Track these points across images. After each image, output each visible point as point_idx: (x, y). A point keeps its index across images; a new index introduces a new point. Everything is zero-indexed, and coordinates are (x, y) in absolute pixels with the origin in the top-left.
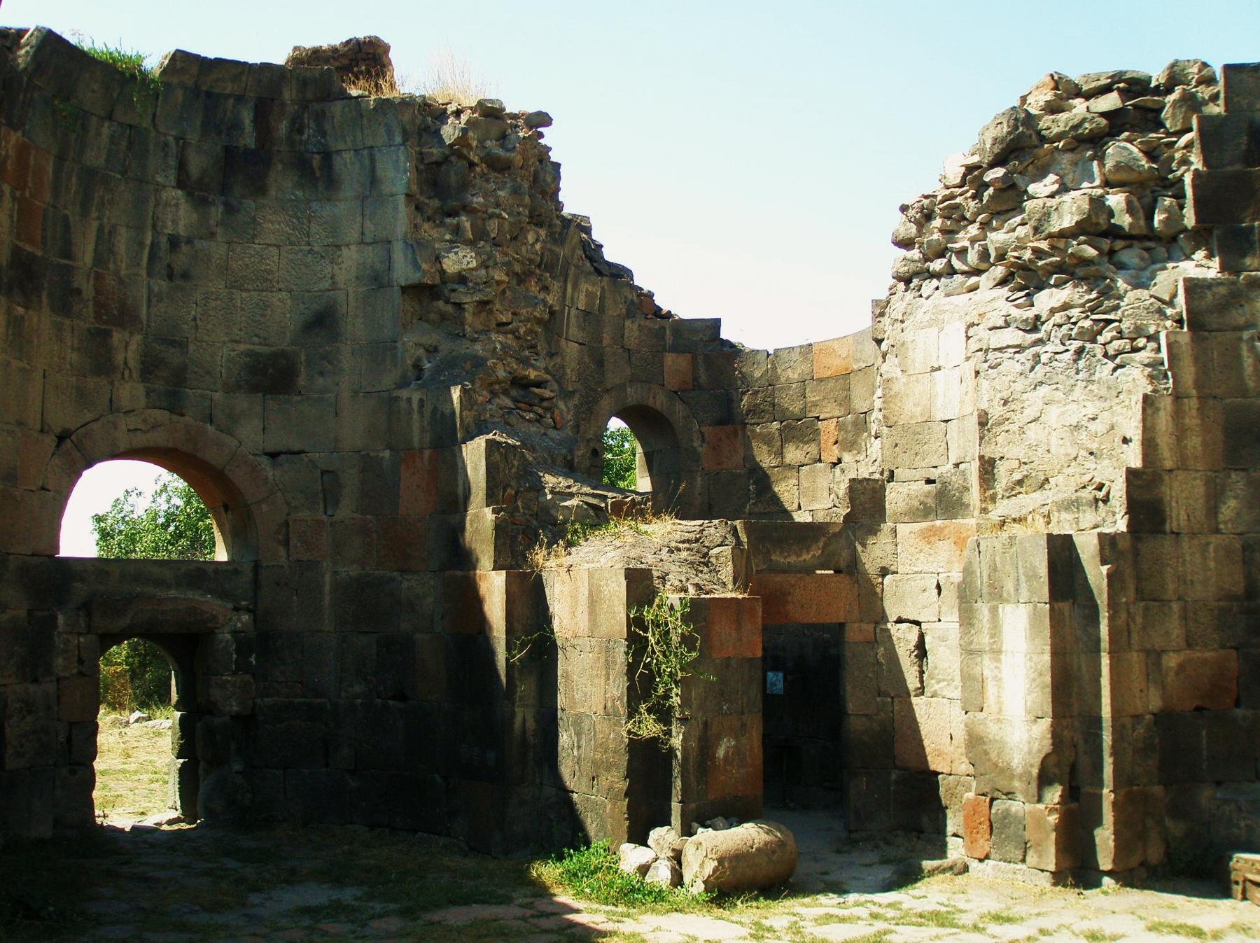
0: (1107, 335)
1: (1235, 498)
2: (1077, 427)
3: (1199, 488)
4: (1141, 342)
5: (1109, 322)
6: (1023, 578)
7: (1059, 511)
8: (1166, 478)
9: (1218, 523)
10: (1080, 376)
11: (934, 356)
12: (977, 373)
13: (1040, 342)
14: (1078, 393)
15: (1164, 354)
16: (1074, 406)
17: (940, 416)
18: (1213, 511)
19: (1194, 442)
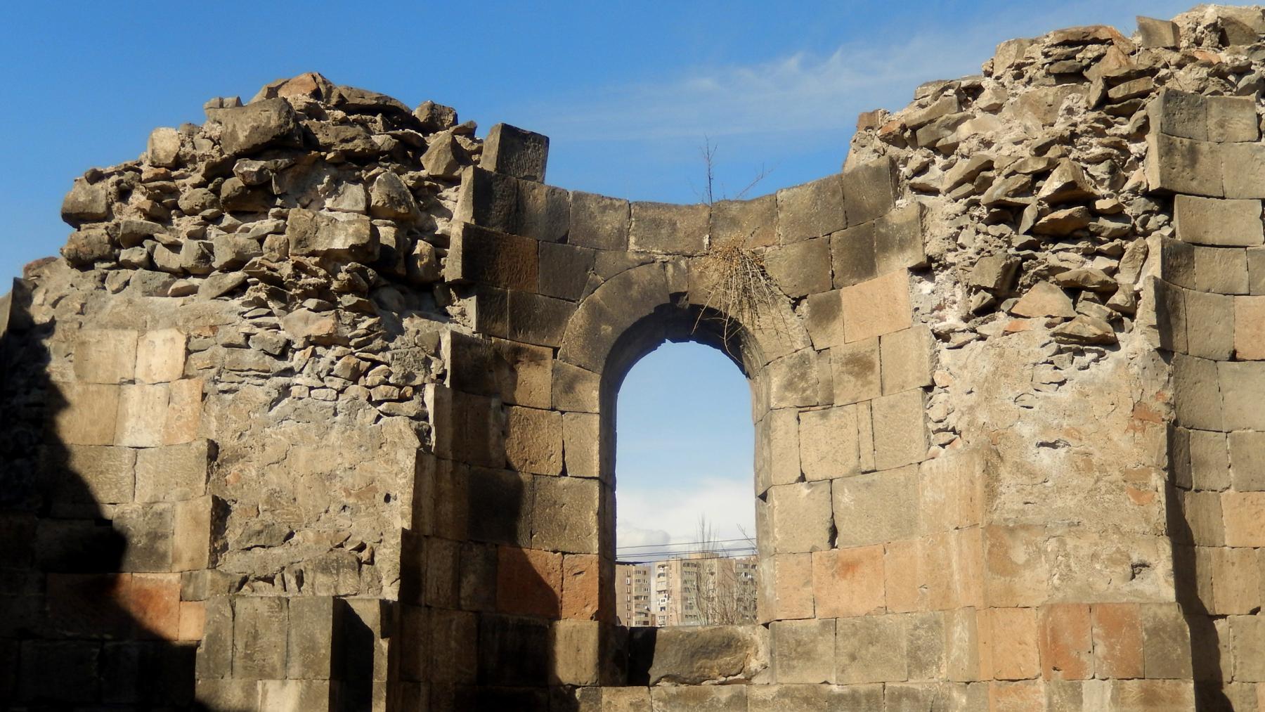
0: (374, 376)
1: (474, 572)
2: (331, 476)
3: (449, 562)
4: (408, 391)
5: (375, 363)
6: (295, 650)
7: (314, 571)
8: (425, 545)
9: (459, 598)
10: (338, 418)
11: (130, 366)
12: (204, 395)
13: (289, 372)
14: (334, 436)
15: (430, 408)
16: (328, 452)
17: (128, 440)
18: (457, 585)
19: (447, 508)
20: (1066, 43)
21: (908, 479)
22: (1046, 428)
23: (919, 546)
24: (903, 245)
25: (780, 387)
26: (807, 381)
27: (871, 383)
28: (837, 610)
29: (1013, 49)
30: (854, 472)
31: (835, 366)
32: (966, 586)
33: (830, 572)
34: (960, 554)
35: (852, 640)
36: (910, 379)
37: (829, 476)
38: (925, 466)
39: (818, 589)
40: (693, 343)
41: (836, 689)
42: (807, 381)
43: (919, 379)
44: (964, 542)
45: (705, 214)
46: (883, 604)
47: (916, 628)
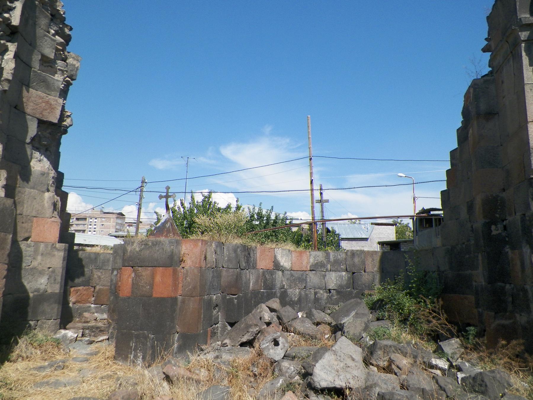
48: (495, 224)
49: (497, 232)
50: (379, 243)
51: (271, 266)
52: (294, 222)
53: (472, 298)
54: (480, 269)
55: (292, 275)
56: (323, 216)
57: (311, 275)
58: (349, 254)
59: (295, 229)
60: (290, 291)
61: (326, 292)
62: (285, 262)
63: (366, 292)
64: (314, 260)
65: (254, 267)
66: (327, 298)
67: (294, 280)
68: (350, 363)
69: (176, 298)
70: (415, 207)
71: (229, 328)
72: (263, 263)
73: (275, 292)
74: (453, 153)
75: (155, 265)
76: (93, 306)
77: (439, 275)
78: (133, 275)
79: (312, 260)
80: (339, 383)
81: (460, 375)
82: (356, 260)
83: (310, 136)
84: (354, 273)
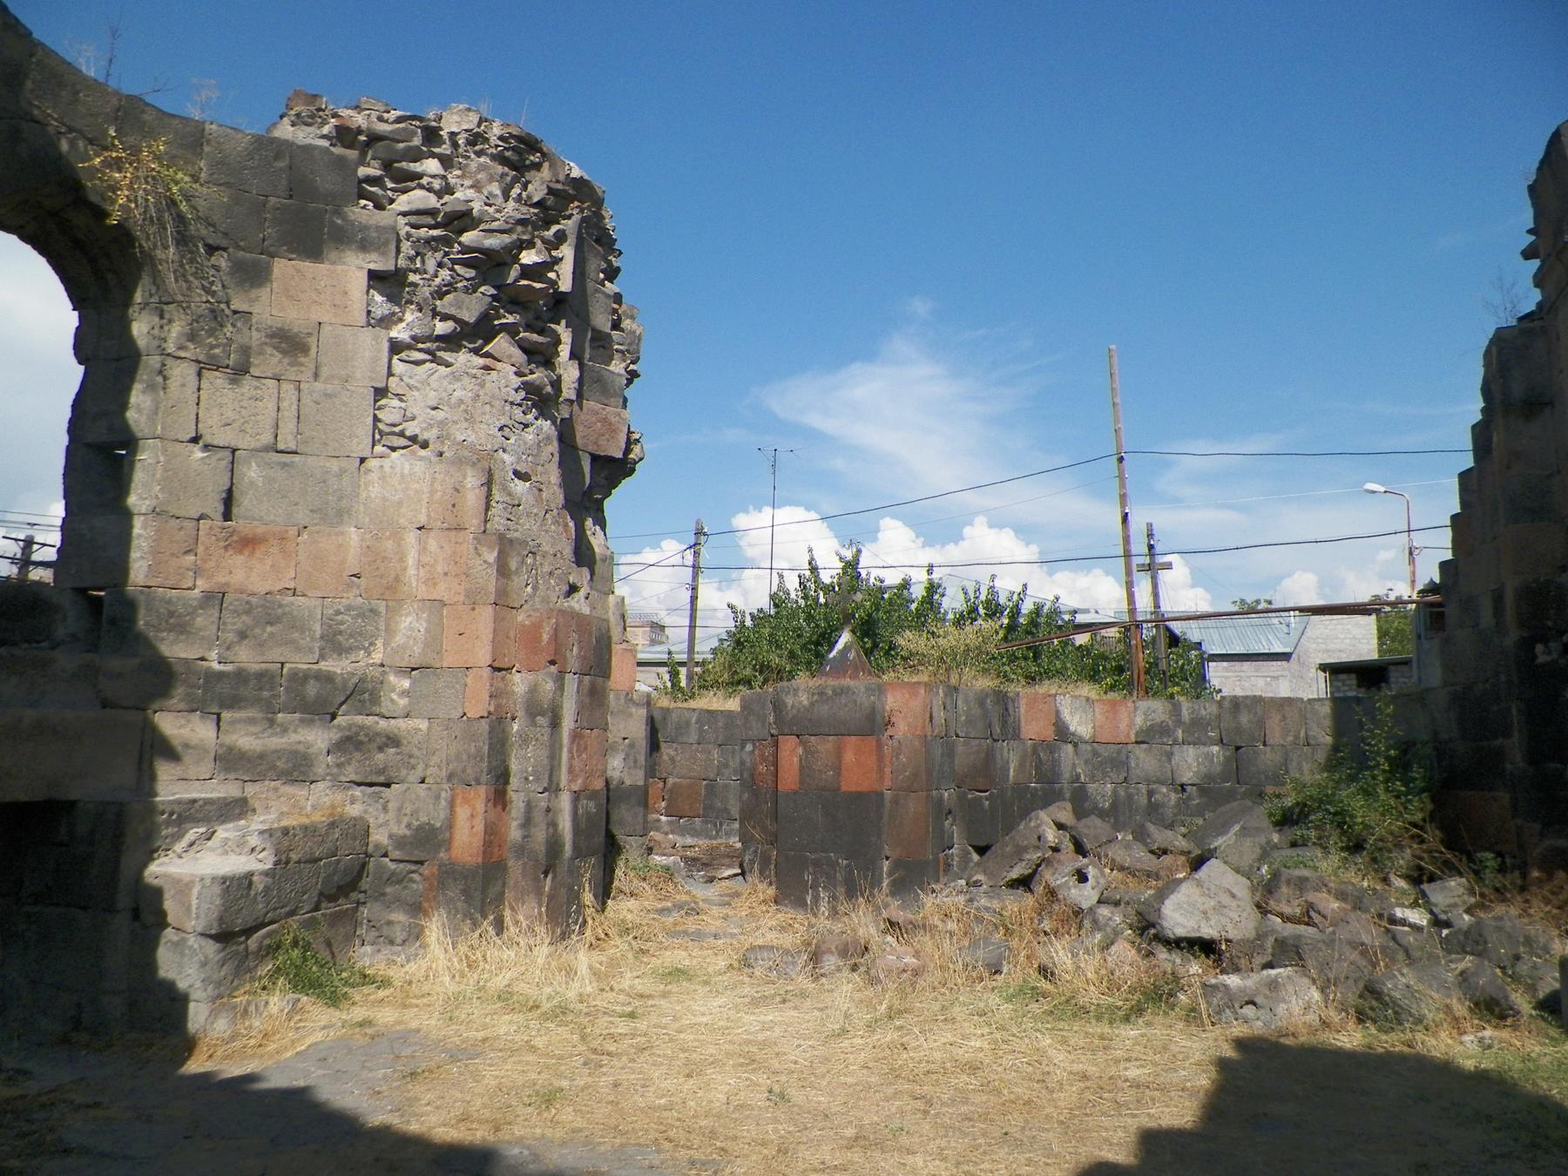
20: (519, 139)
21: (343, 471)
22: (519, 460)
23: (353, 535)
24: (364, 246)
25: (180, 335)
26: (216, 338)
27: (302, 365)
28: (227, 584)
29: (474, 118)
30: (266, 449)
31: (255, 334)
32: (431, 582)
33: (222, 544)
34: (423, 550)
35: (244, 617)
36: (358, 375)
37: (233, 444)
38: (372, 463)
39: (204, 561)
40: (13, 239)
41: (216, 666)
42: (216, 338)
43: (372, 379)
44: (433, 545)
45: (115, 101)
46: (291, 585)
47: (338, 613)
48: (1544, 640)
49: (1549, 658)
50: (1323, 667)
51: (1049, 734)
52: (1080, 618)
53: (1504, 797)
54: (1516, 734)
55: (1095, 754)
56: (1157, 606)
57: (1139, 752)
58: (1226, 704)
59: (1082, 639)
60: (1092, 788)
61: (1176, 791)
62: (1079, 724)
63: (1269, 790)
64: (1145, 720)
65: (1016, 736)
66: (1178, 804)
67: (1101, 763)
68: (1226, 899)
69: (882, 794)
70: (1414, 573)
71: (976, 857)
72: (1034, 728)
73: (1061, 790)
74: (1464, 477)
75: (841, 731)
76: (663, 818)
77: (1436, 749)
78: (800, 750)
79: (1139, 720)
80: (1208, 931)
81: (1445, 932)
82: (1244, 719)
83: (1118, 400)
84: (1238, 748)
